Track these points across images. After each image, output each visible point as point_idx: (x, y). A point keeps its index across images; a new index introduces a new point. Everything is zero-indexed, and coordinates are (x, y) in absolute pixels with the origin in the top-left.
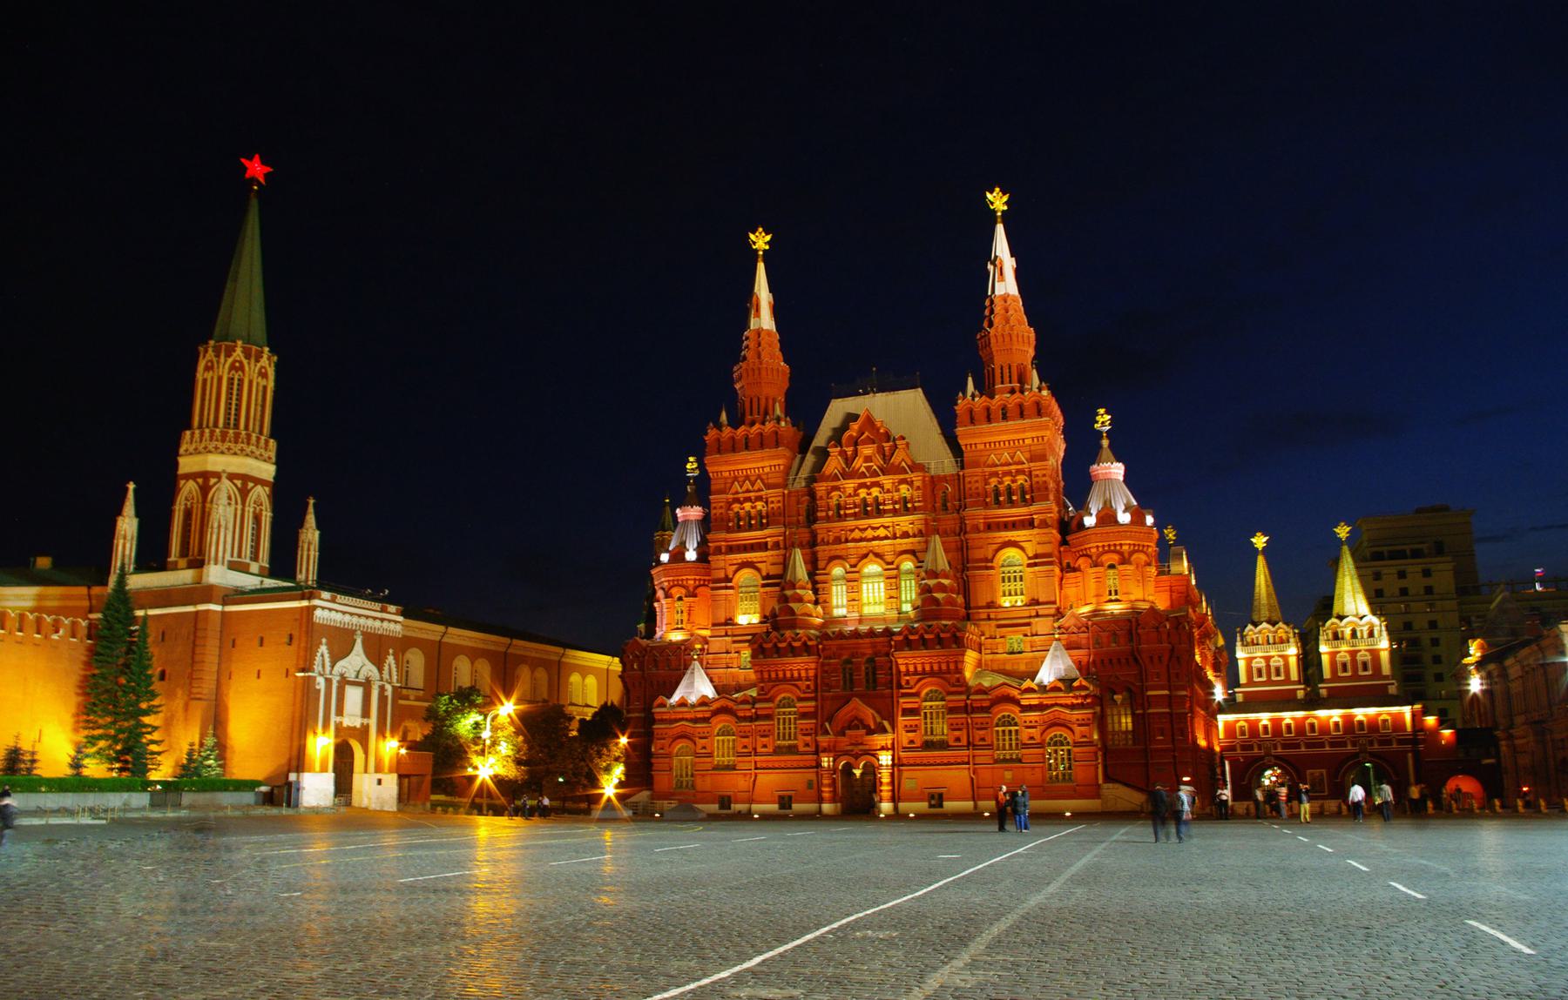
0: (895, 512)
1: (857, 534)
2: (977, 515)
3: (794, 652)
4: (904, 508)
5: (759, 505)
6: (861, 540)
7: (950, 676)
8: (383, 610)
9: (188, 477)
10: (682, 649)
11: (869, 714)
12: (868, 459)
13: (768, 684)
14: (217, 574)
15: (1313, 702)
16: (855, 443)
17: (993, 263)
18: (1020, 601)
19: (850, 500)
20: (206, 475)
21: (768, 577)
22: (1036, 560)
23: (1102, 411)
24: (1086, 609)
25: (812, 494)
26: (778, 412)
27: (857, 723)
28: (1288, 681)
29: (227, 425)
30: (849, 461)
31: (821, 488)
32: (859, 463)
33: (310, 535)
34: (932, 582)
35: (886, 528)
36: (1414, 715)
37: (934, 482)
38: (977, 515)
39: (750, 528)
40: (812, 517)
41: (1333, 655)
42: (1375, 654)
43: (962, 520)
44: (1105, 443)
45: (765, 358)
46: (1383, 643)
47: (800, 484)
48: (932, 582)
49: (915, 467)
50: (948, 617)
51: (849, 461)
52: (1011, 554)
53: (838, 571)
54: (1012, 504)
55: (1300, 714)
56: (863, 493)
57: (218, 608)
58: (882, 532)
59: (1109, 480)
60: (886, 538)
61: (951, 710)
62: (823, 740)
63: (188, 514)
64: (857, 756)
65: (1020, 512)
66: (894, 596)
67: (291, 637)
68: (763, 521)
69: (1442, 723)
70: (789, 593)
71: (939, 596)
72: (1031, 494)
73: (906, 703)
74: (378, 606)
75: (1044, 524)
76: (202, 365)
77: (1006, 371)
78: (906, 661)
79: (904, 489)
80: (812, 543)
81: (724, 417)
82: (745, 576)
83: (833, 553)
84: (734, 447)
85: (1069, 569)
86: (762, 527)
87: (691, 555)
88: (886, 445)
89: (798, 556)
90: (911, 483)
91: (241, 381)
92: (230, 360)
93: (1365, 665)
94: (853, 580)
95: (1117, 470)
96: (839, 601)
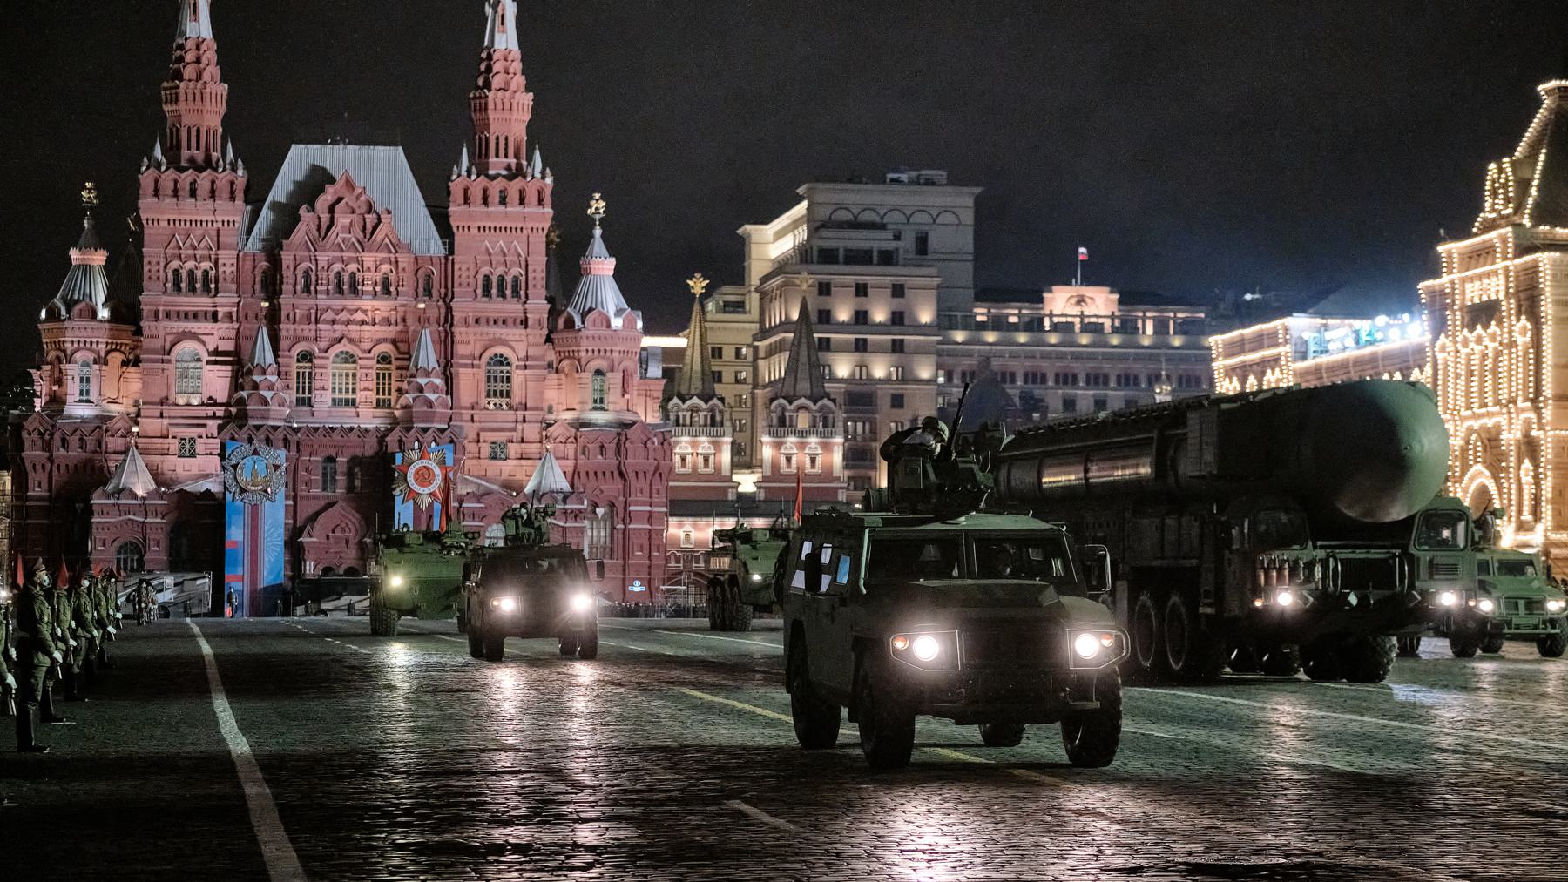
1: (329, 315)
16: (331, 210)
17: (495, 12)
23: (597, 196)
26: (230, 155)
31: (287, 257)
32: (332, 234)
35: (365, 311)
40: (272, 284)
44: (598, 232)
45: (206, 76)
47: (254, 245)
48: (422, 381)
58: (359, 316)
60: (363, 323)
70: (257, 378)
71: (432, 397)
77: (502, 142)
80: (273, 318)
81: (158, 152)
83: (299, 333)
87: (104, 313)
89: (264, 334)
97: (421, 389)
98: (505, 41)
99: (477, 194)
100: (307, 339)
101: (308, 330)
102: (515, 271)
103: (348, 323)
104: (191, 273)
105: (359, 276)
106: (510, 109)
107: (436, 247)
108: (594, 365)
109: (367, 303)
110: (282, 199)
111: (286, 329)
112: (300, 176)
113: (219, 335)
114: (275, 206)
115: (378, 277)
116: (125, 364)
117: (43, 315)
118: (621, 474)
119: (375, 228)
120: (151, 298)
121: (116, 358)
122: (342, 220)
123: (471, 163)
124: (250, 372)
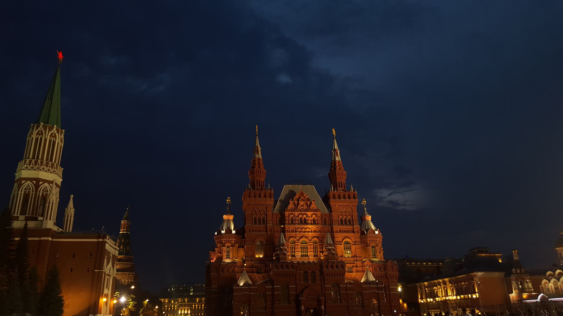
0: (311, 224)
1: (299, 230)
2: (336, 227)
4: (314, 222)
6: (300, 232)
8: (115, 245)
9: (27, 179)
14: (50, 224)
16: (298, 200)
19: (296, 218)
20: (38, 180)
29: (47, 159)
31: (287, 213)
33: (71, 210)
34: (330, 248)
43: (332, 228)
48: (330, 248)
49: (317, 210)
57: (50, 239)
58: (308, 230)
60: (309, 232)
63: (26, 196)
65: (350, 227)
67: (91, 255)
70: (282, 248)
74: (114, 243)
76: (35, 132)
80: (283, 230)
87: (234, 232)
91: (54, 142)
92: (51, 133)
97: (330, 250)
98: (338, 159)
99: (337, 196)
100: (293, 237)
101: (293, 234)
102: (349, 217)
103: (305, 232)
104: (259, 219)
105: (307, 218)
107: (326, 211)
108: (372, 244)
109: (310, 226)
110: (283, 199)
112: (287, 193)
114: (281, 201)
115: (312, 218)
116: (239, 247)
117: (216, 233)
118: (386, 277)
119: (310, 205)
120: (248, 225)
121: (237, 245)
122: (302, 203)
123: (334, 188)
124: (279, 246)
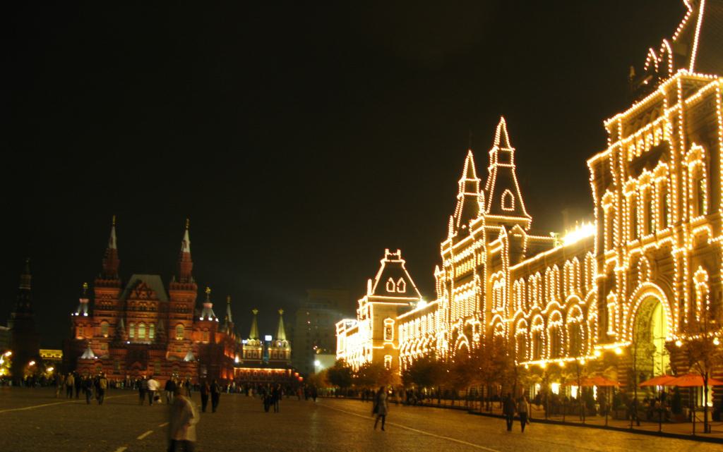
0: (150, 311)
3: (120, 347)
4: (152, 310)
5: (110, 303)
7: (163, 358)
10: (84, 342)
11: (140, 365)
12: (144, 295)
13: (112, 356)
15: (264, 366)
16: (141, 290)
18: (181, 338)
21: (111, 324)
22: (187, 328)
24: (198, 342)
25: (126, 302)
27: (137, 368)
28: (258, 358)
30: (138, 295)
31: (129, 301)
32: (141, 296)
36: (292, 372)
37: (161, 304)
38: (172, 315)
39: (106, 309)
40: (125, 309)
41: (272, 351)
42: (284, 352)
44: (208, 297)
46: (288, 349)
49: (157, 299)
50: (163, 340)
51: (138, 295)
52: (181, 326)
53: (132, 325)
54: (183, 313)
55: (259, 369)
56: (141, 304)
58: (146, 316)
59: (208, 308)
61: (162, 366)
62: (128, 372)
64: (136, 376)
65: (184, 315)
66: (147, 334)
68: (110, 308)
69: (300, 375)
71: (161, 336)
72: (187, 311)
73: (151, 364)
75: (190, 319)
78: (151, 353)
79: (153, 305)
80: (125, 317)
81: (100, 276)
82: (104, 323)
84: (103, 286)
85: (195, 330)
86: (110, 310)
88: (149, 292)
90: (154, 303)
93: (281, 356)
94: (136, 328)
95: (210, 305)
96: (132, 333)
98: (187, 250)
106: (188, 266)
111: (128, 319)
113: (111, 319)
121: (89, 325)
